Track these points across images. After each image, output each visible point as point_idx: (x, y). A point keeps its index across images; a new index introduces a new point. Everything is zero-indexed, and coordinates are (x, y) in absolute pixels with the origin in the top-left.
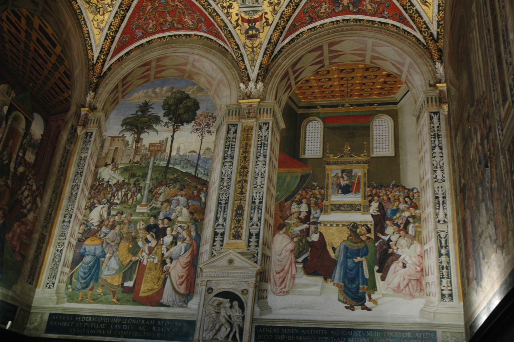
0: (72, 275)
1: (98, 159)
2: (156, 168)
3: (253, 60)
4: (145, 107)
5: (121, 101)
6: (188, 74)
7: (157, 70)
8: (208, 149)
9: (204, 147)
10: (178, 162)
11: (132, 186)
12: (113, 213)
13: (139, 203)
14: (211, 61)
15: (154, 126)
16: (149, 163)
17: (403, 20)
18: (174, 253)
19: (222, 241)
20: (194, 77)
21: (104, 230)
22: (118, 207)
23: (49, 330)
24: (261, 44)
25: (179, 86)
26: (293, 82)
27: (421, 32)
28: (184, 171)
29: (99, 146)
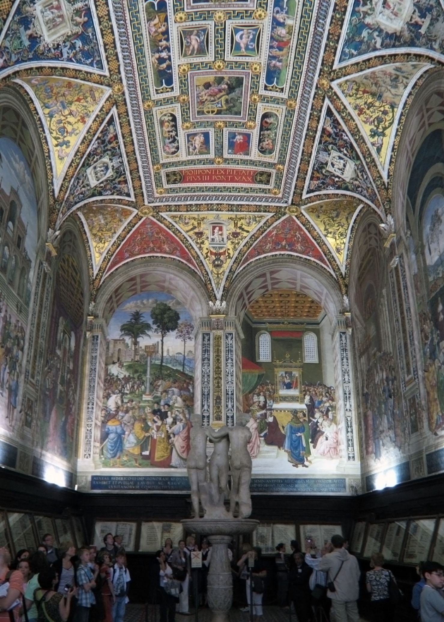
0: (102, 448)
1: (107, 358)
2: (153, 366)
3: (218, 284)
4: (137, 316)
5: (117, 310)
6: (166, 290)
7: (142, 285)
8: (190, 352)
9: (187, 351)
10: (169, 361)
11: (136, 380)
12: (125, 401)
13: (144, 393)
14: (184, 280)
15: (146, 331)
16: (147, 362)
17: (322, 260)
18: (175, 430)
19: (209, 422)
20: (173, 292)
21: (120, 414)
22: (129, 396)
23: (93, 487)
24: (224, 272)
25: (162, 299)
26: (247, 302)
27: (334, 271)
28: (175, 368)
29: (105, 347)
